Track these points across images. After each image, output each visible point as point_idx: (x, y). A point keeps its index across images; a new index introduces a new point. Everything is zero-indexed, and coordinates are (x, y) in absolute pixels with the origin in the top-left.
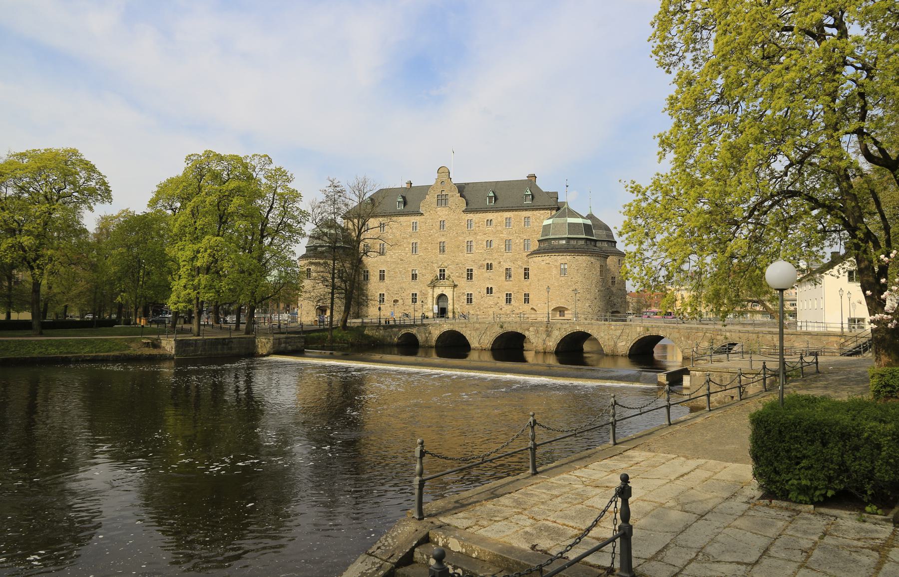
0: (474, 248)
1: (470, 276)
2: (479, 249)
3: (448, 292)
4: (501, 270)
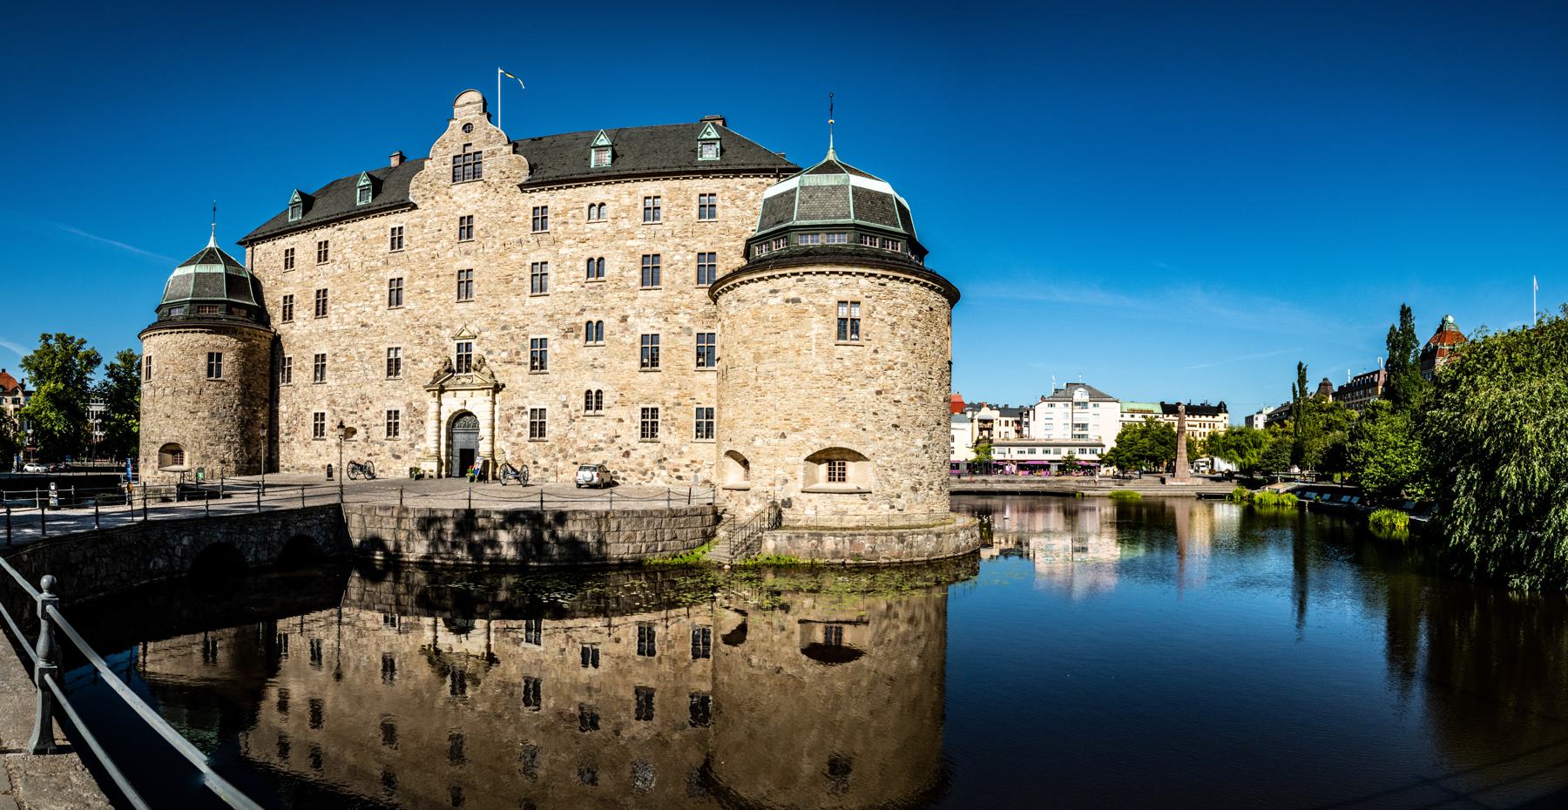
0: (551, 282)
1: (538, 362)
2: (566, 279)
3: (479, 404)
4: (628, 339)
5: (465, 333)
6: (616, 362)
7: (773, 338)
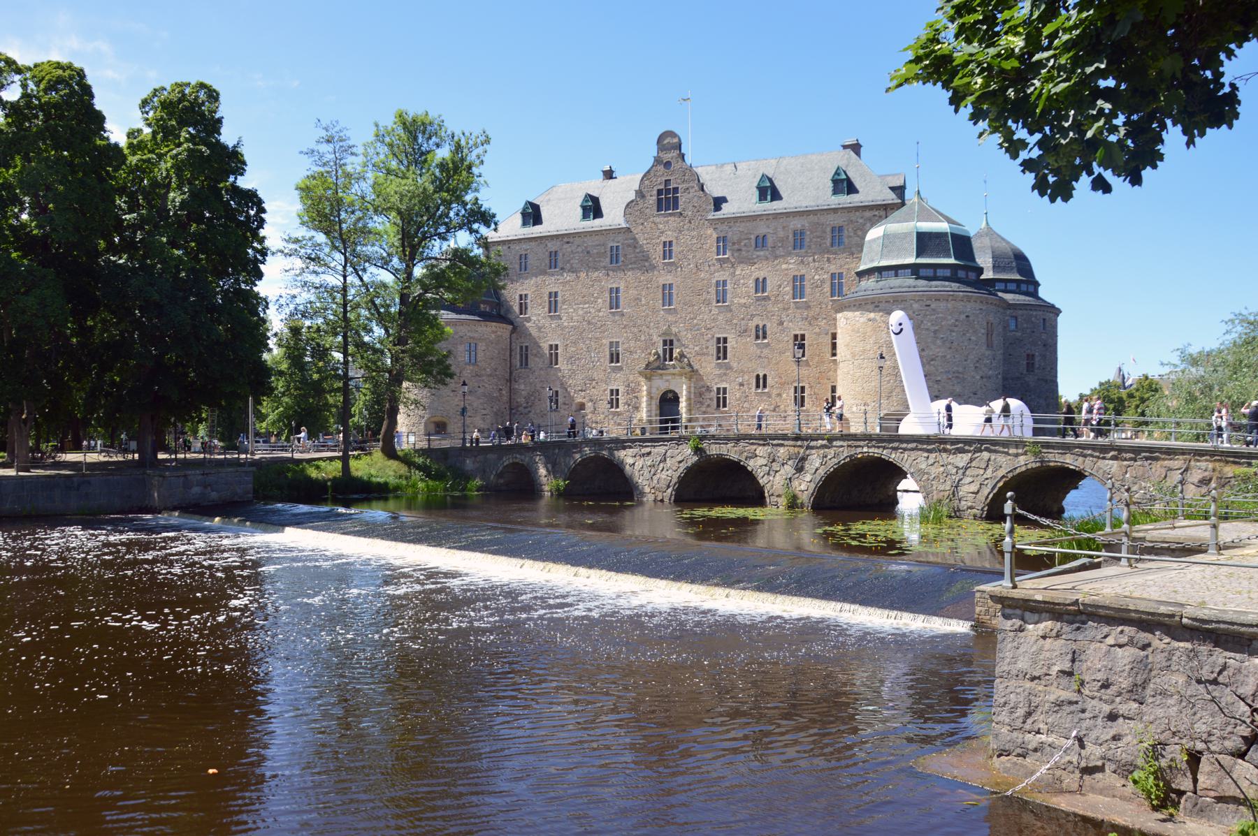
1: (722, 352)
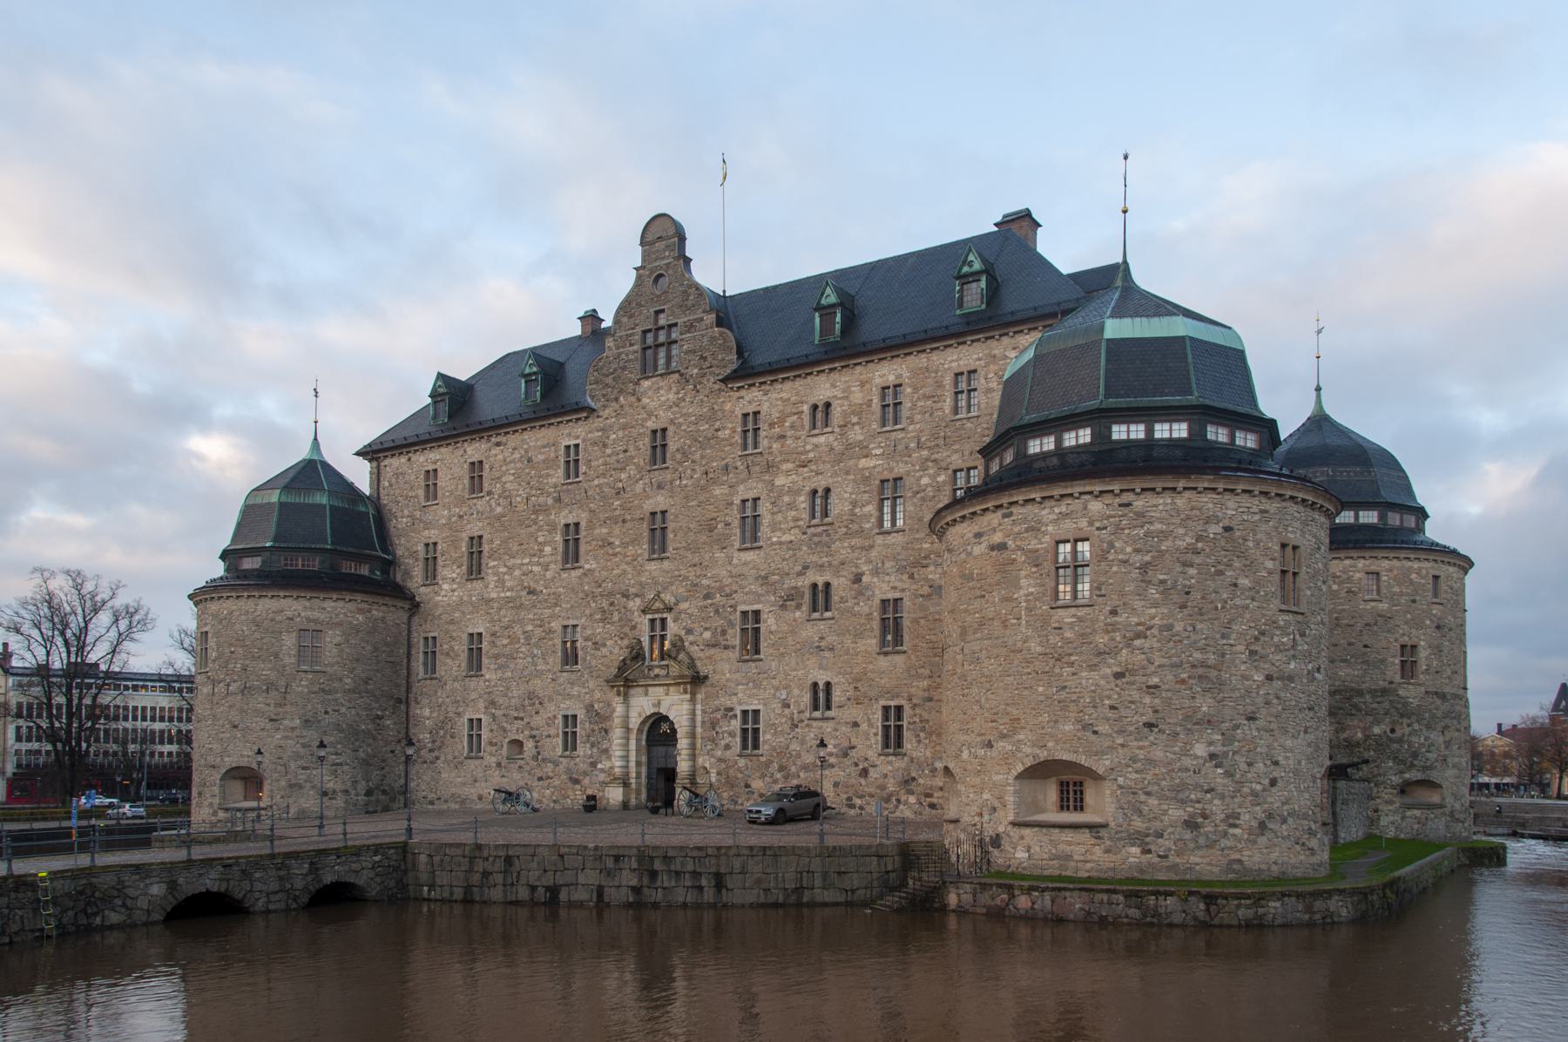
0: (764, 530)
1: (752, 642)
3: (676, 706)
4: (863, 608)
5: (658, 605)
6: (848, 641)
7: (977, 604)
